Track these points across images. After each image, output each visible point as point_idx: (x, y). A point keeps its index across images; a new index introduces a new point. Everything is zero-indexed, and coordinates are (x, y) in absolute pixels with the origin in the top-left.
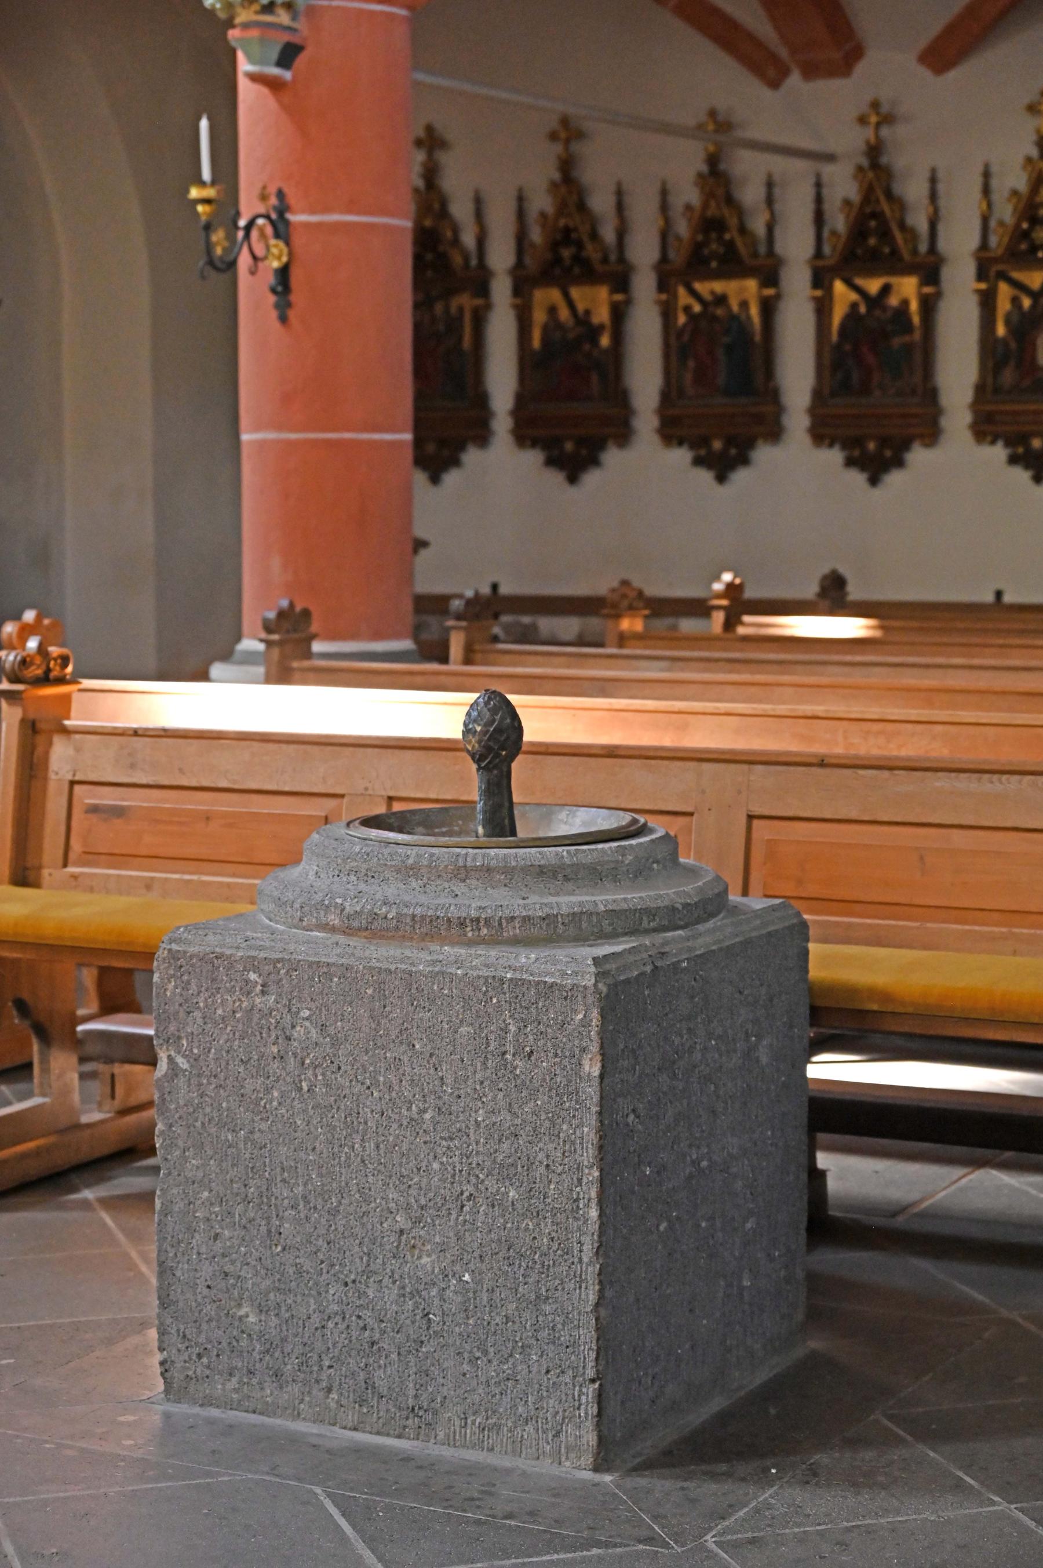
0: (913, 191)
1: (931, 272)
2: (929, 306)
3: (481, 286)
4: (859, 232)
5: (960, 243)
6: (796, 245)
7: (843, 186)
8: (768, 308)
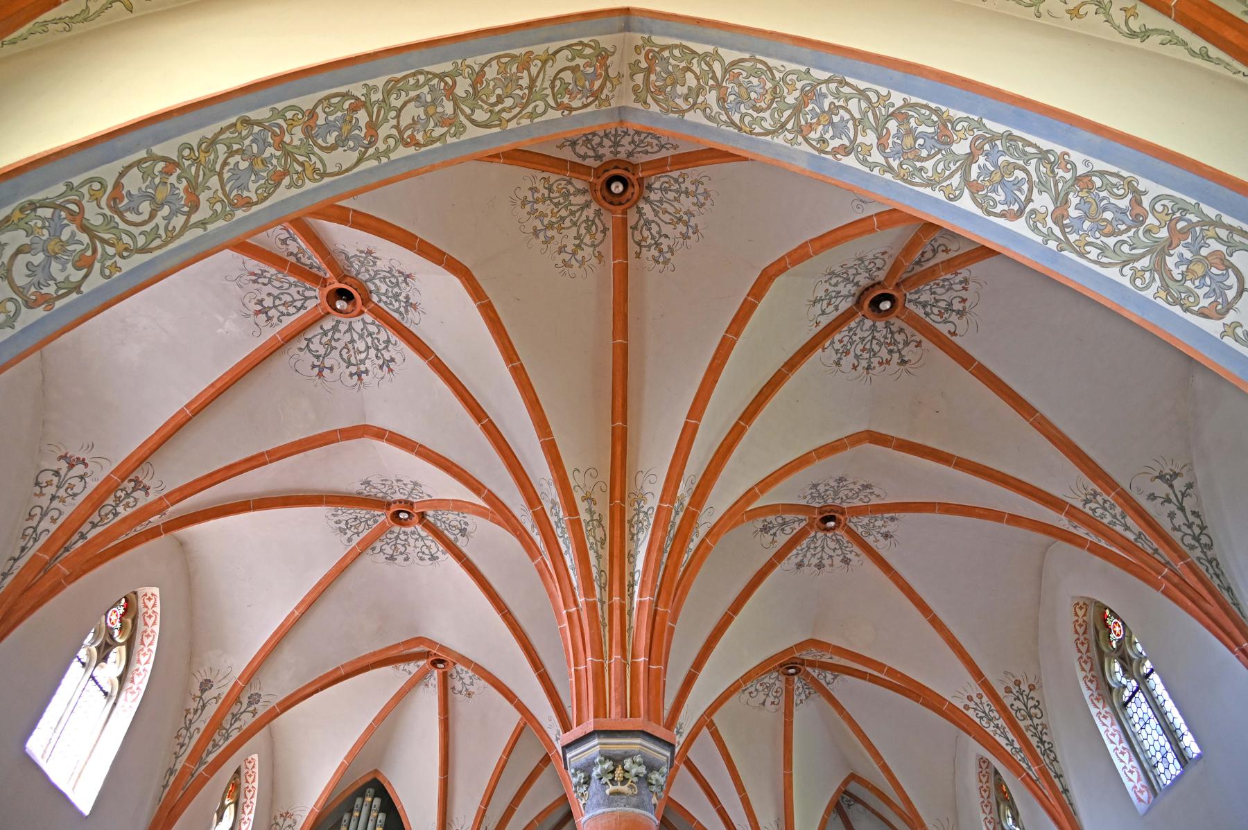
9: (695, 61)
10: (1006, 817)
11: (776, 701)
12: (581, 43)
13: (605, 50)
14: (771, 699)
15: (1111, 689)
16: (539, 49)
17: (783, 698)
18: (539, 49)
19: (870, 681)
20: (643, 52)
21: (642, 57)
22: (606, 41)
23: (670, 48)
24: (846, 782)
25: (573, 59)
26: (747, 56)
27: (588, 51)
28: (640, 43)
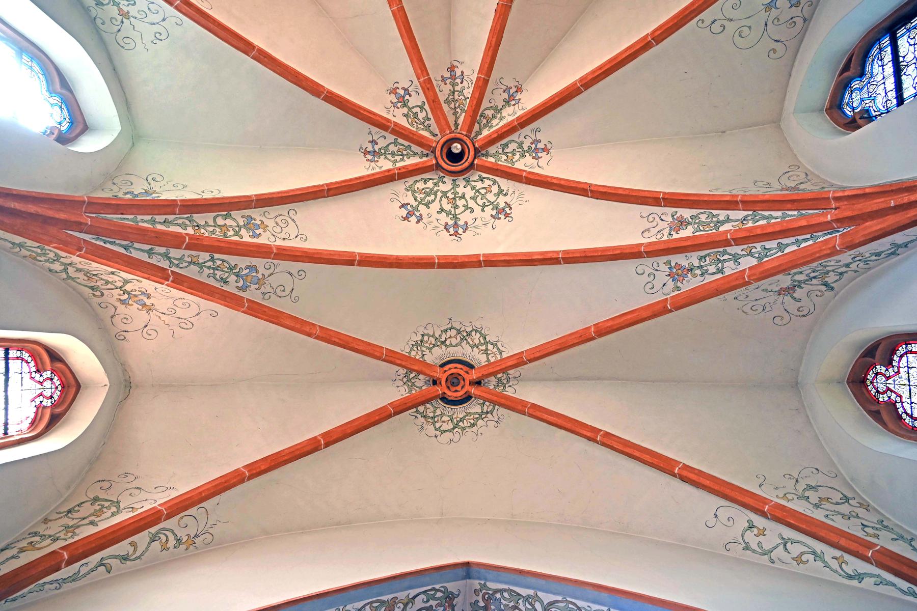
9: (520, 601)
12: (434, 589)
13: (452, 593)
16: (402, 595)
18: (402, 595)
20: (481, 594)
21: (480, 598)
22: (452, 587)
23: (502, 591)
25: (428, 601)
26: (560, 598)
27: (439, 595)
28: (478, 587)
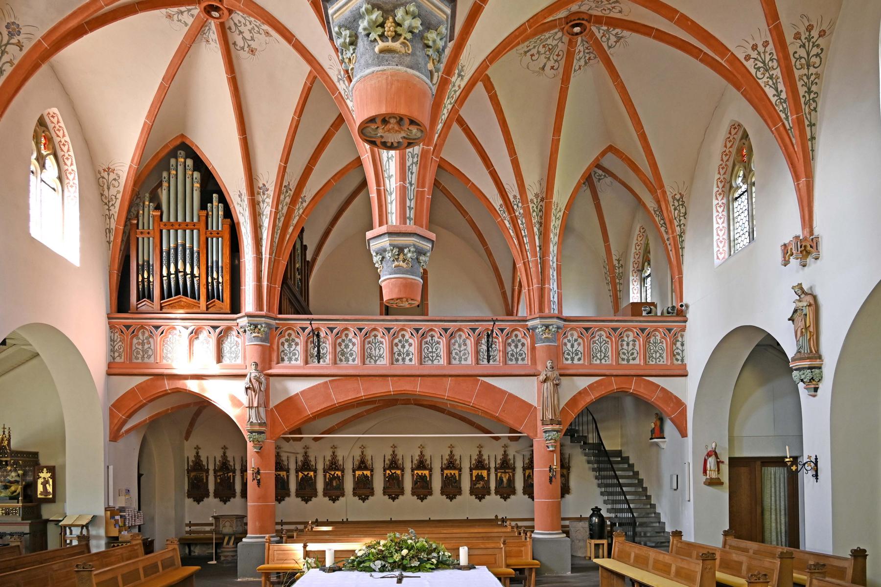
0: (312, 459)
1: (315, 471)
2: (315, 476)
3: (234, 471)
4: (303, 465)
5: (320, 467)
6: (292, 467)
7: (300, 458)
8: (288, 476)
10: (737, 176)
11: (556, 65)
14: (551, 63)
15: (731, 187)
17: (563, 62)
19: (655, 38)
24: (603, 154)
